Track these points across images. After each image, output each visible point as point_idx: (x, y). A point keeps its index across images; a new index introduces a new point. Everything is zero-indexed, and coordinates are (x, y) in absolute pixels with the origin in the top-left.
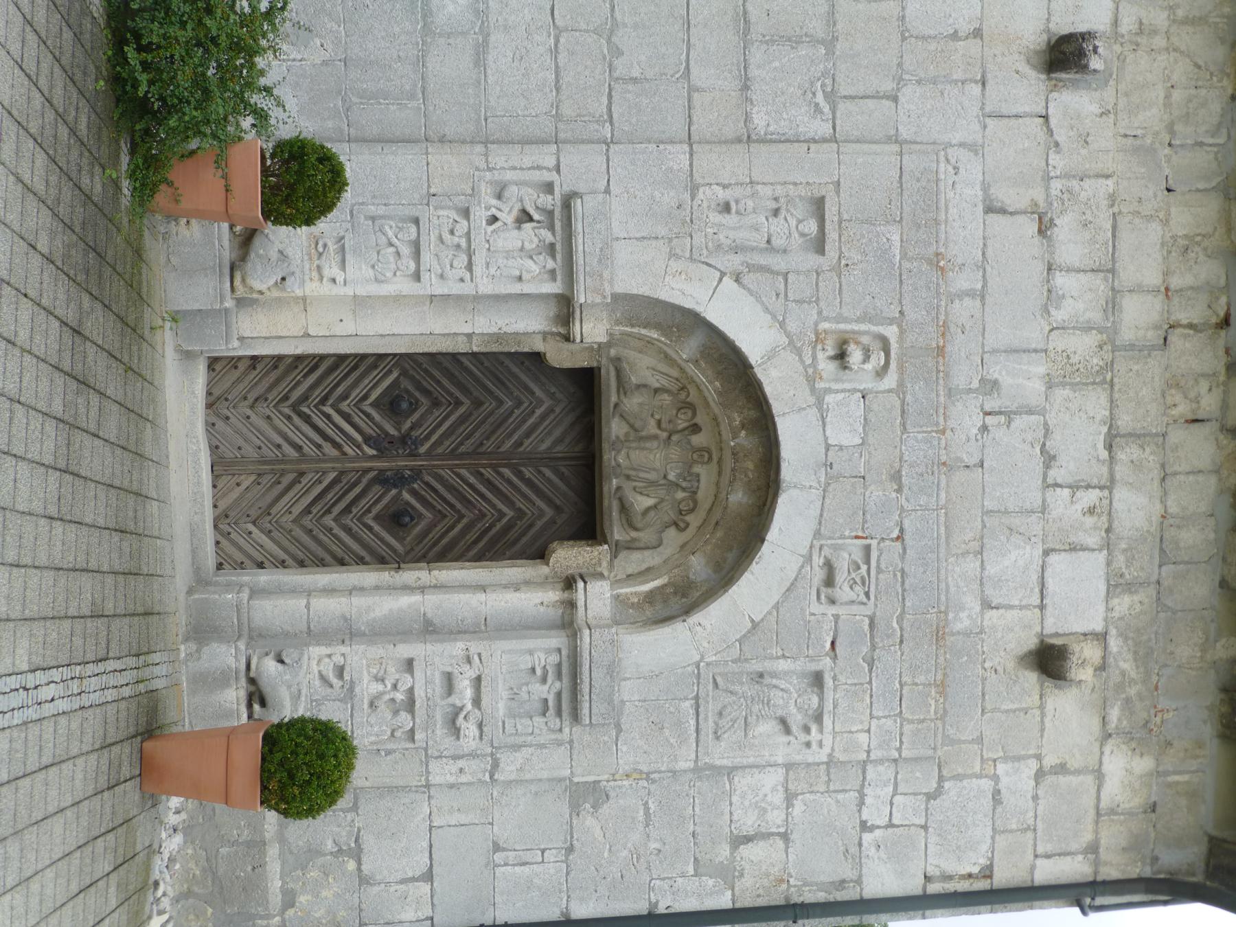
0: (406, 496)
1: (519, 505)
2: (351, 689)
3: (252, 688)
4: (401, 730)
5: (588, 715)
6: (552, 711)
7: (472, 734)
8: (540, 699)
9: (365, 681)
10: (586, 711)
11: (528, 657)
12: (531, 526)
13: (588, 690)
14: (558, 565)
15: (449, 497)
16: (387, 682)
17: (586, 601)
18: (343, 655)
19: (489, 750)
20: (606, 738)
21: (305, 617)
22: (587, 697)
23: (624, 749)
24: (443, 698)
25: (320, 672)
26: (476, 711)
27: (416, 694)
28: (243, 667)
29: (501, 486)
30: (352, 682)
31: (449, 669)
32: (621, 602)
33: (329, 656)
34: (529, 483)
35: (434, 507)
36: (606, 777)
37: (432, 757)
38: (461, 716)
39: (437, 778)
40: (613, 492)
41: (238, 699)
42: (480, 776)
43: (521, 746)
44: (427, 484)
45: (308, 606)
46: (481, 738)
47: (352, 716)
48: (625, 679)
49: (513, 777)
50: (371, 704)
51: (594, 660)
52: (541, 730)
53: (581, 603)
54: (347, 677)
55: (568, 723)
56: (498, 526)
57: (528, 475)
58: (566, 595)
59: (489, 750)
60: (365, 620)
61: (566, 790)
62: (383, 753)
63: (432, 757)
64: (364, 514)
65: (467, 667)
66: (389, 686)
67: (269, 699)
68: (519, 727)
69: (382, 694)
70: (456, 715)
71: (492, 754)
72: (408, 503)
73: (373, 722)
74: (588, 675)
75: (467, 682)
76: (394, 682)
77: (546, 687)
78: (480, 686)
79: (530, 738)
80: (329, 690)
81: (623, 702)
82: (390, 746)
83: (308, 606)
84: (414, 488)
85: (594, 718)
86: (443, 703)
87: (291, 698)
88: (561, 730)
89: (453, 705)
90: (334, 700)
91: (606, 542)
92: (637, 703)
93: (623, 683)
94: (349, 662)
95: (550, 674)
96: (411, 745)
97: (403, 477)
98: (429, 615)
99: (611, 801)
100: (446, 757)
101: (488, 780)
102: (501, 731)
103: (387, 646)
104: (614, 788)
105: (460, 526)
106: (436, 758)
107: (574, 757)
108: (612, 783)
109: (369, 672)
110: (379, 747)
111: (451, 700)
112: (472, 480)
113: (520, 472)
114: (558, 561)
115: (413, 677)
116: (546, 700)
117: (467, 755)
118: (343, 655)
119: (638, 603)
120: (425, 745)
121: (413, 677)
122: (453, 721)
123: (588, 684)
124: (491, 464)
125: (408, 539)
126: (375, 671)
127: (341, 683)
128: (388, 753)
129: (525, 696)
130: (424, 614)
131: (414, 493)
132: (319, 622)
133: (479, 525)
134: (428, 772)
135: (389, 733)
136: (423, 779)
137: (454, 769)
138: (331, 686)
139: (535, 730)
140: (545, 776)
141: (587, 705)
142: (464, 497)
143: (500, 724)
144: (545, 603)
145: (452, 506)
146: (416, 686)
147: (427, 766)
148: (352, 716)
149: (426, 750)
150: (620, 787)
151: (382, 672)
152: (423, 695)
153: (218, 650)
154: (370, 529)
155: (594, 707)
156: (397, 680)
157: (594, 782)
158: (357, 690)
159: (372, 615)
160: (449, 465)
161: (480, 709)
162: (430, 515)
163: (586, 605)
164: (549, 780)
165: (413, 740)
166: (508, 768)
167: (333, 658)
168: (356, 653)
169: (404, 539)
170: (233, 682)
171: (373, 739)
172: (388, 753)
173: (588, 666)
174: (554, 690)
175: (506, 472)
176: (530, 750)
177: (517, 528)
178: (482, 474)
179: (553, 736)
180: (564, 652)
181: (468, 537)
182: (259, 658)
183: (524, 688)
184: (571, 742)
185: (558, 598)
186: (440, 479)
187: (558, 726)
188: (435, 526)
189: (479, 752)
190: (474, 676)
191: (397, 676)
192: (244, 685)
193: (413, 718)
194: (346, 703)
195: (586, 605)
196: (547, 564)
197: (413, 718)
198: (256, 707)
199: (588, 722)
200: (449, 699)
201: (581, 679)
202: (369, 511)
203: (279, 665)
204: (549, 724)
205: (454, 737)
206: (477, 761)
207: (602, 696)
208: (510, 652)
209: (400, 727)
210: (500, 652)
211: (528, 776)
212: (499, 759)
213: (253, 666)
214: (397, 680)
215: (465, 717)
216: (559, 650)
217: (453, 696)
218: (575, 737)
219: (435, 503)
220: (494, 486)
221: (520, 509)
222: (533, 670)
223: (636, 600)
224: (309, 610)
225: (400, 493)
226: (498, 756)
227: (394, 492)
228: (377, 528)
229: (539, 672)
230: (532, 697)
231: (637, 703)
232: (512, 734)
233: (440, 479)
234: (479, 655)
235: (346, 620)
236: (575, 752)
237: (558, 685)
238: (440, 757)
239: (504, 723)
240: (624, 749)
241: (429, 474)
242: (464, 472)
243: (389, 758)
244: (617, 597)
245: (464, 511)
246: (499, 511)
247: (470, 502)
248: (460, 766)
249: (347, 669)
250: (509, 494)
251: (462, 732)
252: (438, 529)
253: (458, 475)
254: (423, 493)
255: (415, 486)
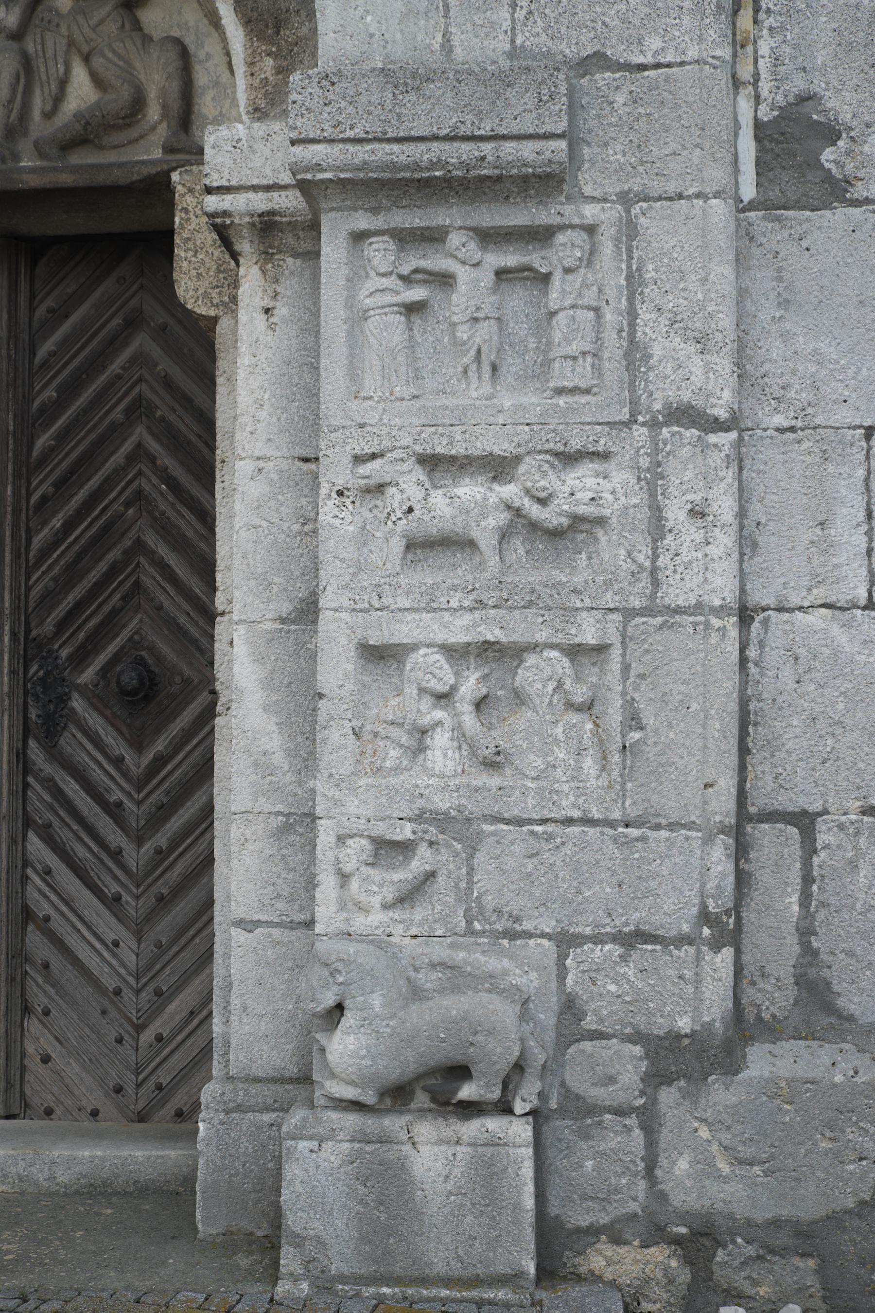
0: (88, 675)
1: (117, 414)
2: (442, 820)
3: (421, 1099)
4: (568, 684)
5: (538, 145)
6: (536, 259)
7: (590, 482)
8: (495, 290)
9: (422, 781)
10: (528, 150)
11: (372, 325)
12: (168, 384)
13: (465, 147)
14: (214, 294)
15: (94, 576)
16: (426, 721)
17: (255, 188)
18: (341, 839)
19: (640, 433)
20: (620, 98)
21: (276, 932)
22: (487, 148)
23: (654, 43)
24: (481, 566)
25: (385, 907)
26: (522, 469)
27: (463, 638)
28: (351, 1120)
29: (74, 455)
30: (419, 818)
31: (397, 545)
32: (272, 103)
33: (344, 878)
34: (69, 391)
35: (114, 613)
36: (745, 106)
37: (653, 596)
38: (535, 511)
39: (718, 582)
40: (45, 163)
41: (441, 1142)
42: (716, 458)
43: (632, 340)
44: (61, 626)
45: (248, 925)
46: (604, 456)
47: (519, 822)
48: (447, 46)
49: (724, 364)
50: (492, 765)
51: (377, 129)
52: (585, 285)
53: (259, 202)
54: (406, 832)
55: (568, 209)
56: (167, 461)
57: (51, 393)
58: (245, 247)
59: (640, 433)
60: (290, 778)
61: (778, 219)
62: (636, 735)
63: (653, 596)
64: (125, 775)
65: (394, 498)
66: (439, 714)
67: (457, 1056)
68: (574, 348)
69: (460, 735)
70: (534, 526)
71: (654, 425)
72: (105, 671)
73: (539, 763)
74: (422, 147)
75: (438, 499)
76: (426, 703)
77: (463, 273)
78: (453, 459)
79: (609, 316)
80: (441, 879)
81: (512, 54)
82: (614, 716)
83: (248, 925)
84: (70, 657)
85: (549, 127)
86: (493, 561)
87: (456, 990)
88: (591, 230)
89: (504, 535)
90: (471, 871)
91: (167, 174)
92: (520, 14)
93: (459, 53)
94: (362, 825)
95: (423, 263)
96: (616, 652)
97: (43, 681)
98: (286, 608)
99: (819, 87)
100: (655, 556)
101: (733, 435)
102: (584, 399)
103: (321, 717)
104: (778, 80)
105: (163, 551)
106: (656, 583)
107: (672, 188)
108: (765, 87)
109: (396, 770)
110: (616, 746)
111: (487, 541)
112: (57, 522)
113: (42, 410)
114: (206, 295)
115: (414, 647)
116: (501, 274)
117: (652, 494)
118: (341, 839)
119: (275, 56)
120: (616, 617)
121: (414, 647)
122: (556, 534)
123: (446, 146)
124: (17, 476)
125: (187, 672)
126: (394, 753)
127: (423, 850)
128: (633, 721)
129: (486, 331)
130: (283, 620)
131: (81, 658)
132: (290, 900)
133: (163, 506)
134: (698, 608)
135: (574, 718)
136: (716, 622)
137: (692, 533)
138: (431, 875)
139: (585, 301)
140: (728, 271)
141: (509, 147)
142: (94, 541)
143: (561, 401)
144: (267, 302)
145: (114, 570)
146: (441, 637)
147: (678, 611)
148: (519, 822)
149: (629, 614)
150: (777, 61)
151: (395, 732)
152: (466, 619)
153: (299, 1188)
154: (160, 761)
155: (515, 128)
156: (422, 691)
157: (757, 138)
158: (442, 803)
159: (278, 759)
160: (15, 577)
161: (517, 459)
162: (135, 621)
163: (268, 188)
164: (741, 262)
165: (601, 649)
166: (698, 379)
167: (348, 868)
168: (336, 802)
169: (187, 681)
170: (391, 1153)
171: (589, 764)
172: (633, 721)
173: (396, 147)
174: (473, 251)
175: (42, 442)
176: (645, 314)
177: (172, 418)
178: (44, 499)
179: (607, 248)
180: (362, 221)
181: (190, 534)
182: (333, 1076)
183: (463, 333)
184: (626, 199)
185: (255, 270)
186: (49, 598)
187: (579, 237)
188: (160, 608)
189: (644, 462)
190: (420, 474)
191: (411, 691)
192: (404, 1120)
193: (534, 647)
194: (480, 835)
195: (268, 188)
196: (215, 320)
197: (534, 647)
198: (467, 1092)
199: (563, 144)
200: (482, 544)
201: (432, 166)
202: (117, 762)
203: (349, 1019)
204: (568, 263)
205: (600, 533)
206: (671, 466)
207: (484, 106)
208: (354, 374)
209: (560, 685)
210: (354, 405)
211: (726, 320)
212: (668, 405)
213: (350, 1093)
214: (422, 691)
215: (543, 502)
216: (359, 237)
217: (475, 534)
218: (612, 188)
219: (107, 608)
220: (71, 472)
221: (129, 411)
222: (412, 309)
223: (269, 62)
224: (258, 923)
225: (82, 690)
226: (657, 406)
227: (77, 703)
228: (160, 745)
229: (417, 294)
230: (486, 310)
231: (520, 14)
232: (597, 370)
233: (49, 598)
234: (359, 460)
235: (286, 829)
236: (656, 187)
237: (455, 239)
238: (654, 571)
239: (560, 391)
240: (654, 43)
241: (42, 622)
242: (37, 542)
243: (649, 720)
244: (258, 113)
245: (127, 543)
246: (131, 458)
247: (106, 529)
248: (682, 515)
249: (381, 829)
250: (93, 436)
251: (582, 510)
252: (166, 604)
253: (44, 554)
254: (82, 635)
255: (65, 653)
